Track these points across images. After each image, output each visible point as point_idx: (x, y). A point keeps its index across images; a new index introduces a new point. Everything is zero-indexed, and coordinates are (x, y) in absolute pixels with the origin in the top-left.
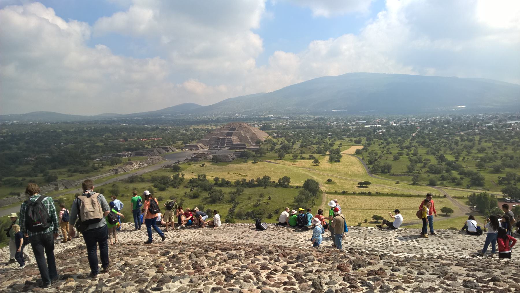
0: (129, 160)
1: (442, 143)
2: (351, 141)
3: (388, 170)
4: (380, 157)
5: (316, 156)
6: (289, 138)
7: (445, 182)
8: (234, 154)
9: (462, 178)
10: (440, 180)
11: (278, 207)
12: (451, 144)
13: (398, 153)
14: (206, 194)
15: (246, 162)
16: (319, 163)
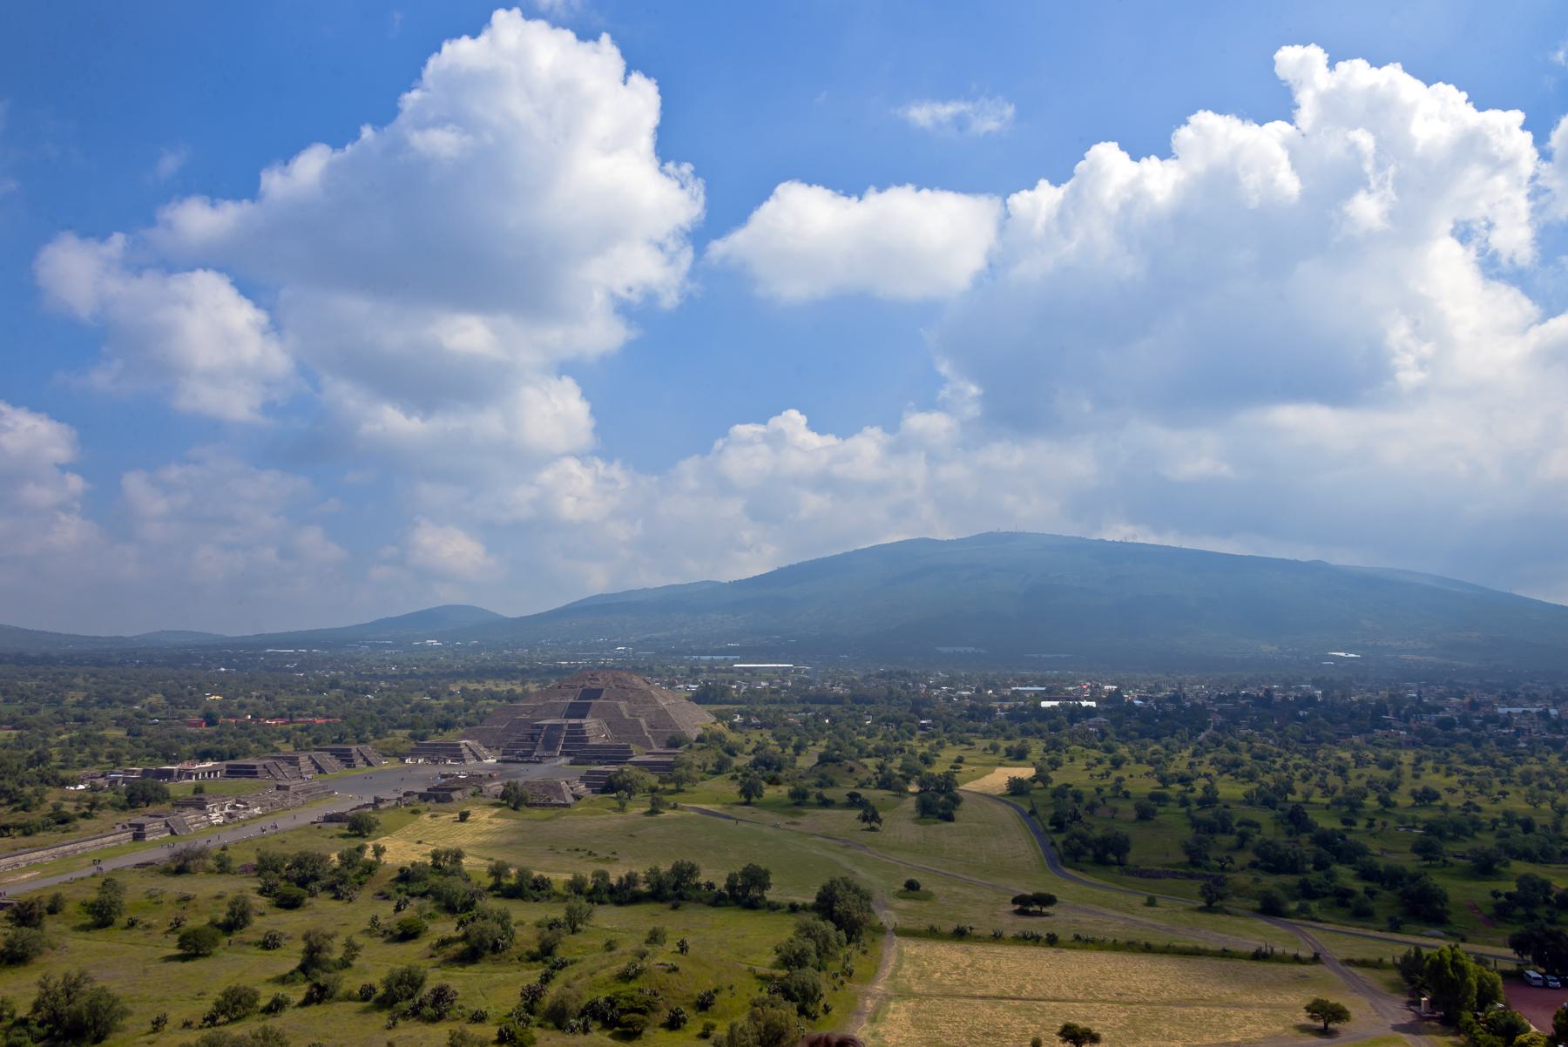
0: (199, 790)
1: (1297, 767)
2: (995, 749)
3: (1118, 854)
4: (1091, 808)
5: (873, 794)
6: (785, 732)
7: (1314, 905)
8: (582, 779)
9: (1370, 893)
10: (1295, 898)
11: (711, 985)
12: (1324, 774)
13: (1153, 797)
14: (446, 927)
16: (880, 821)
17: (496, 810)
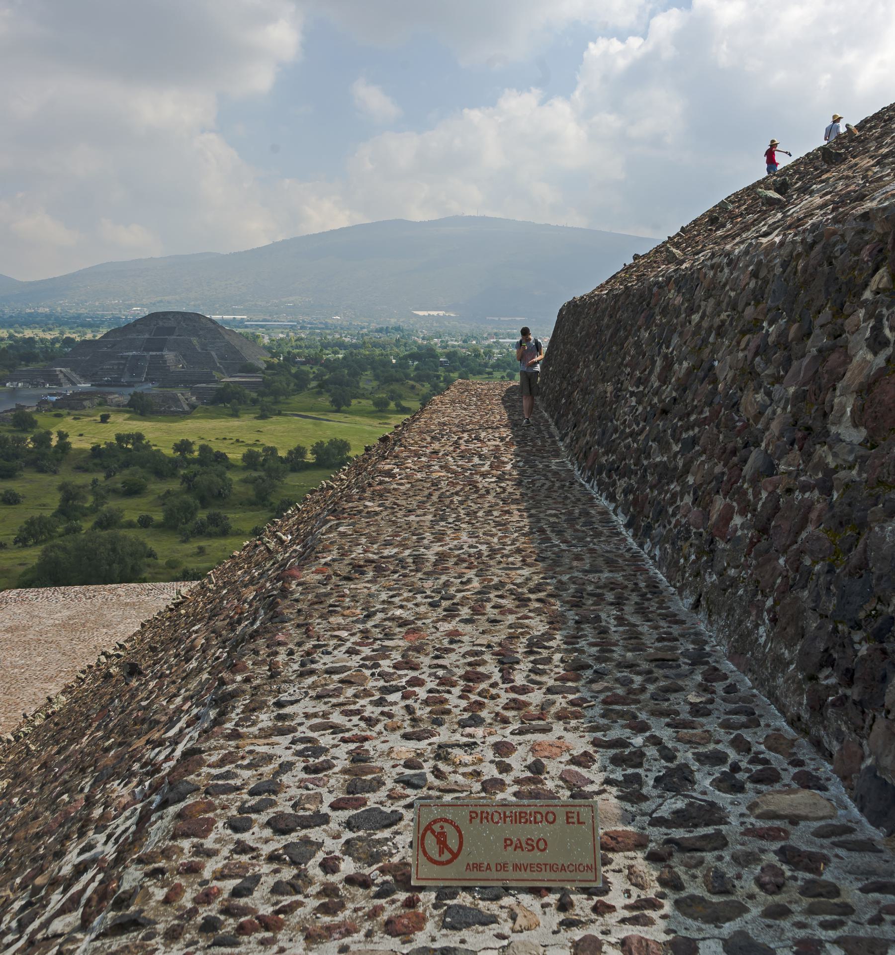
15: (235, 414)
17: (127, 415)
